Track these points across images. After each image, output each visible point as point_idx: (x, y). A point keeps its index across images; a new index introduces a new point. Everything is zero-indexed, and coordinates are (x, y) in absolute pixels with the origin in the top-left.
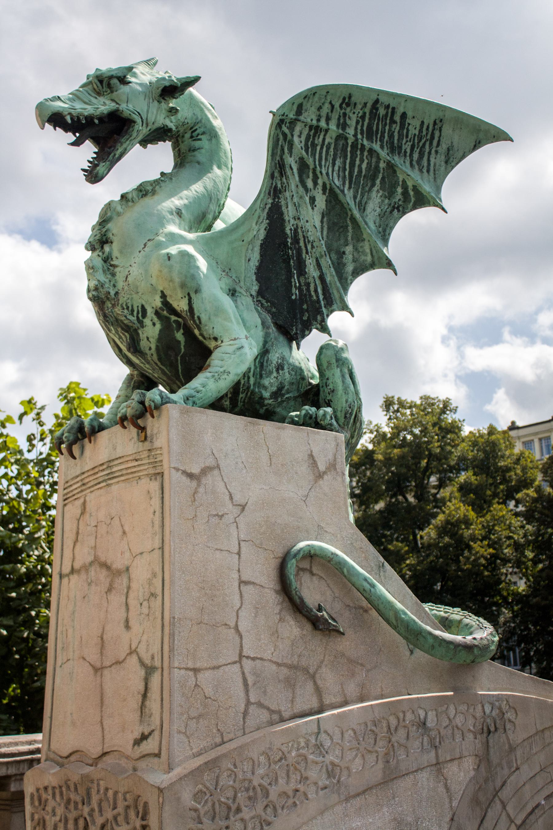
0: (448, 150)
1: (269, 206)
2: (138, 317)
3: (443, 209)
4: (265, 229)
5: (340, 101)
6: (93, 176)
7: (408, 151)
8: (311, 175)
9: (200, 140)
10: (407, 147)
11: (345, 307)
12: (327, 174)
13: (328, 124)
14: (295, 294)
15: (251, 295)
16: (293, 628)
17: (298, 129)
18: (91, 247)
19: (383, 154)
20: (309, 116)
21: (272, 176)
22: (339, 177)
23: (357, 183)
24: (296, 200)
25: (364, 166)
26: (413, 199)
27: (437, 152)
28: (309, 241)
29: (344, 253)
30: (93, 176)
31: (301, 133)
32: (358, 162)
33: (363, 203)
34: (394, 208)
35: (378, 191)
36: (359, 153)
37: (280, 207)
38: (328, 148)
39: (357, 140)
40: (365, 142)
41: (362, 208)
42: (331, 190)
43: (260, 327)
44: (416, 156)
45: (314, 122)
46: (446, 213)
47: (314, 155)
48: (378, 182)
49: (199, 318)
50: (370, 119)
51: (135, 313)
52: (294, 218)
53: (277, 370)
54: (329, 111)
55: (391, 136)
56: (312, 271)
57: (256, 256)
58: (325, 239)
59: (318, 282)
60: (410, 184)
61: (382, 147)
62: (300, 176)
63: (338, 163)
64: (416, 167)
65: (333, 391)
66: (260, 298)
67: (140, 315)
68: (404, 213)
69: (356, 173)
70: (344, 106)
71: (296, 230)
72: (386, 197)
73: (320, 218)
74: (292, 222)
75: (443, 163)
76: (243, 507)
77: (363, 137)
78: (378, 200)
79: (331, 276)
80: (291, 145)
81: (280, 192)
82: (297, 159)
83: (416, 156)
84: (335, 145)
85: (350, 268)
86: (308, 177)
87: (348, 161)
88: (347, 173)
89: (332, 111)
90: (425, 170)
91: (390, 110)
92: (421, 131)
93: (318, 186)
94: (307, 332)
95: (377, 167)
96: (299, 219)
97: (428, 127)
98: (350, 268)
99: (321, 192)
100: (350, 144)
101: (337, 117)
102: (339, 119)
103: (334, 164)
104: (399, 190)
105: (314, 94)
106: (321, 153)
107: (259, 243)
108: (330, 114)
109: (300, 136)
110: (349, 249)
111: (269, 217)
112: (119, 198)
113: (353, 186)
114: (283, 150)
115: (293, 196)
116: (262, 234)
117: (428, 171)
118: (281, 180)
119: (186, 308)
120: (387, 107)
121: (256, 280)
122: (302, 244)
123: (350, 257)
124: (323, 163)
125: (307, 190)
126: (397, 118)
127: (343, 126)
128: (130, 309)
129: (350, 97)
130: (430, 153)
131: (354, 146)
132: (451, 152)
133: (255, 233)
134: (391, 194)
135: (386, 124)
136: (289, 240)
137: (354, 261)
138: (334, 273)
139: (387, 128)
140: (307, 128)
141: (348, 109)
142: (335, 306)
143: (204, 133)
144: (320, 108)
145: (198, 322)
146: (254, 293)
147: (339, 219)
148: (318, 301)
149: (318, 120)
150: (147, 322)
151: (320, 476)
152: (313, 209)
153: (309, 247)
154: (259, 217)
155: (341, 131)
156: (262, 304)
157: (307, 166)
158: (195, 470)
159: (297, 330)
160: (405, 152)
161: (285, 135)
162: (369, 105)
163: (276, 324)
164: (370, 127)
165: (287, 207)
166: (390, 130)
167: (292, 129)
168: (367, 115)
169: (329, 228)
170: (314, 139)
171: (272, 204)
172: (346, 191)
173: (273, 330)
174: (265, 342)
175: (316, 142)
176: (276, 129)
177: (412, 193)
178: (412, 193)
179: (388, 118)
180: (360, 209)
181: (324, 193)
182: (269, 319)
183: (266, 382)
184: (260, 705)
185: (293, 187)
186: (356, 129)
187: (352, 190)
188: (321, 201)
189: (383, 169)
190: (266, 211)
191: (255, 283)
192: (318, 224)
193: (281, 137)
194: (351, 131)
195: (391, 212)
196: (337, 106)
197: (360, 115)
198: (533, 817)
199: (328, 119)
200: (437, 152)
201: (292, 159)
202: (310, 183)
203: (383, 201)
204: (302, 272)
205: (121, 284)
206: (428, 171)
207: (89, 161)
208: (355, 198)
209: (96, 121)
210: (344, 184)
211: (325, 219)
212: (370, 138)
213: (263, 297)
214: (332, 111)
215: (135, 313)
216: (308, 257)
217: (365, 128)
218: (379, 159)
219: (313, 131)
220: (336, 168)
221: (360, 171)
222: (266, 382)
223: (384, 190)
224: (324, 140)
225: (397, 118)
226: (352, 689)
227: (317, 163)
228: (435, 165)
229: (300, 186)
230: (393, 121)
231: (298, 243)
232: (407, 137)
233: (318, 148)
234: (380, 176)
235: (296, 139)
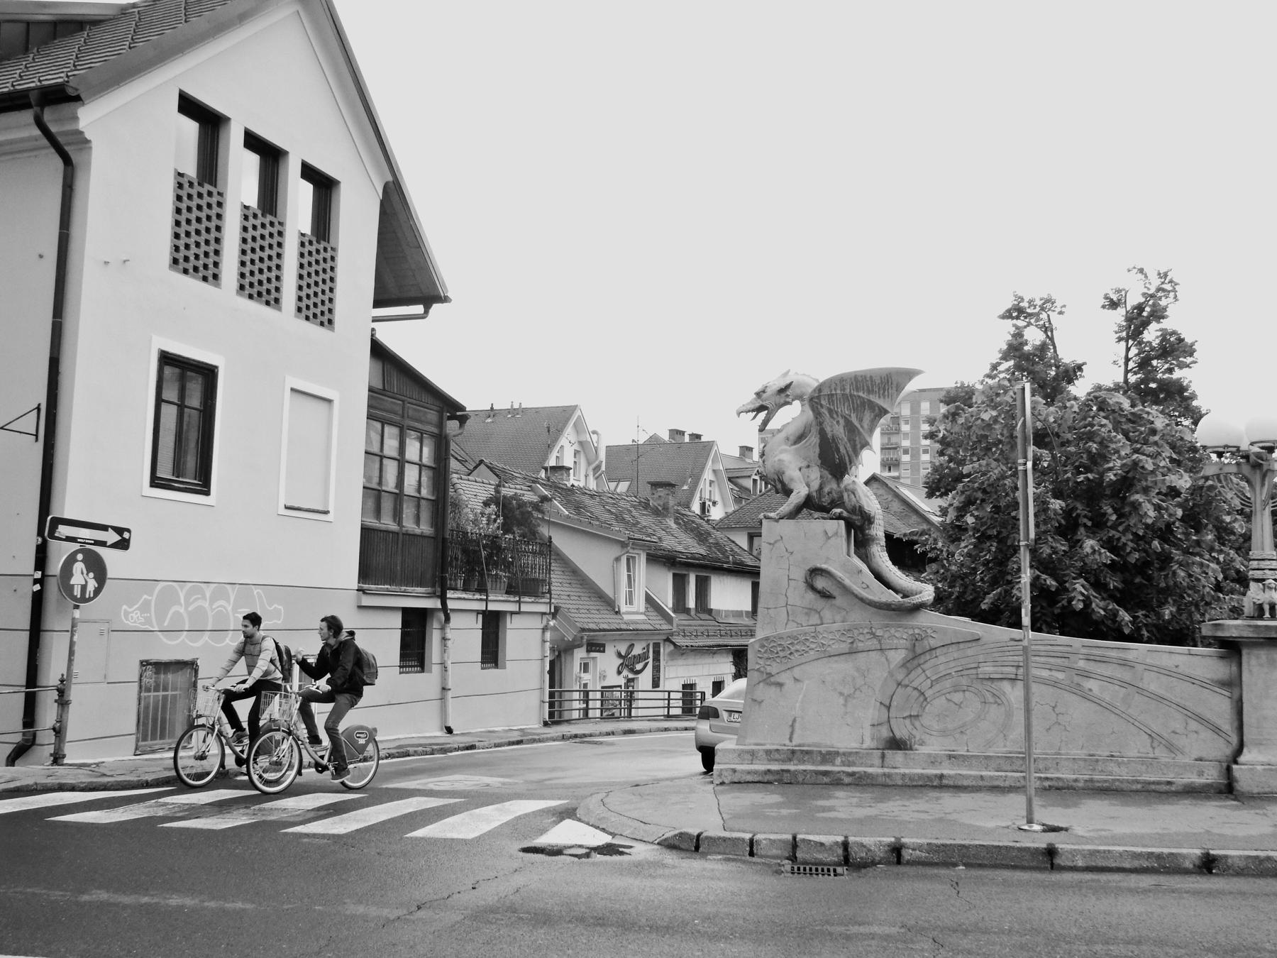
16: (811, 595)
20: (826, 391)
41: (861, 420)
56: (842, 450)
57: (818, 450)
79: (851, 452)
147: (851, 429)
188: (842, 421)
226: (838, 618)
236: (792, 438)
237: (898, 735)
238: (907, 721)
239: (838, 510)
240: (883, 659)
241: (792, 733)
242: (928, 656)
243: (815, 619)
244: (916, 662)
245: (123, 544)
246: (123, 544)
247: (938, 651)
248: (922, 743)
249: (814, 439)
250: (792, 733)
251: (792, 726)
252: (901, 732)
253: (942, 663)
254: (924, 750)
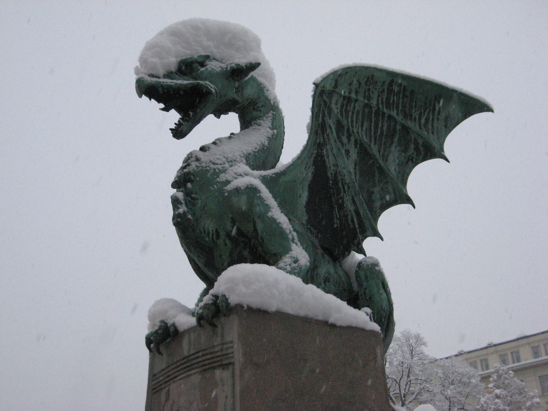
0: (447, 118)
1: (315, 155)
2: (213, 238)
3: (447, 160)
4: (312, 173)
5: (366, 79)
6: (179, 132)
7: (417, 117)
8: (345, 133)
9: (260, 111)
10: (416, 114)
11: (376, 234)
12: (358, 133)
13: (357, 96)
14: (336, 224)
15: (302, 223)
17: (335, 98)
18: (175, 185)
19: (399, 118)
21: (316, 133)
22: (366, 134)
24: (335, 151)
25: (385, 128)
26: (423, 153)
27: (438, 119)
28: (346, 183)
29: (373, 192)
30: (179, 132)
31: (337, 102)
32: (380, 125)
33: (386, 155)
34: (409, 159)
35: (396, 147)
36: (380, 118)
37: (323, 156)
38: (358, 114)
39: (379, 108)
40: (385, 110)
41: (385, 158)
42: (361, 144)
44: (423, 121)
45: (347, 94)
46: (449, 162)
47: (347, 118)
48: (396, 140)
49: (262, 238)
50: (388, 94)
51: (211, 235)
52: (334, 165)
53: (325, 282)
54: (357, 87)
58: (358, 180)
59: (354, 215)
60: (420, 142)
61: (398, 114)
62: (337, 134)
63: (366, 125)
64: (424, 129)
65: (370, 298)
66: (309, 226)
67: (214, 237)
68: (417, 164)
69: (379, 133)
70: (368, 83)
71: (336, 174)
72: (402, 151)
73: (353, 165)
74: (332, 168)
75: (443, 127)
77: (383, 106)
78: (397, 154)
79: (363, 210)
80: (330, 111)
81: (323, 146)
82: (335, 121)
83: (423, 121)
84: (363, 112)
85: (378, 204)
86: (344, 135)
87: (373, 124)
88: (372, 133)
89: (359, 87)
90: (430, 132)
91: (402, 88)
92: (425, 103)
93: (351, 142)
94: (347, 253)
95: (395, 130)
96: (338, 166)
97: (430, 100)
98: (378, 204)
99: (353, 146)
100: (374, 111)
101: (364, 91)
102: (365, 93)
103: (362, 126)
104: (412, 146)
105: (346, 73)
106: (352, 117)
107: (307, 184)
108: (358, 89)
109: (336, 104)
110: (376, 190)
111: (315, 163)
112: (198, 149)
113: (377, 143)
114: (324, 113)
115: (332, 148)
117: (433, 133)
118: (323, 136)
119: (251, 229)
121: (306, 212)
122: (340, 185)
123: (378, 196)
124: (354, 125)
126: (408, 94)
127: (369, 98)
128: (206, 232)
129: (373, 77)
130: (433, 119)
131: (377, 113)
132: (448, 119)
133: (304, 175)
134: (405, 150)
135: (399, 98)
136: (331, 182)
138: (366, 208)
139: (401, 101)
140: (342, 99)
142: (368, 233)
143: (262, 106)
144: (350, 84)
145: (261, 241)
146: (304, 222)
148: (355, 228)
149: (350, 93)
152: (348, 159)
153: (346, 188)
154: (307, 163)
155: (366, 101)
156: (311, 231)
157: (343, 127)
159: (339, 251)
160: (415, 119)
161: (325, 103)
162: (386, 84)
163: (323, 248)
164: (388, 99)
165: (328, 157)
166: (403, 102)
167: (330, 98)
168: (386, 90)
169: (360, 174)
170: (347, 107)
171: (317, 154)
172: (372, 145)
173: (320, 251)
174: (315, 260)
175: (349, 109)
176: (319, 97)
177: (422, 148)
178: (422, 148)
179: (401, 94)
180: (383, 160)
181: (356, 147)
182: (316, 242)
185: (332, 141)
186: (378, 100)
187: (377, 146)
189: (400, 130)
190: (312, 159)
191: (305, 214)
192: (352, 171)
193: (322, 103)
195: (407, 162)
196: (363, 83)
197: (380, 91)
200: (438, 119)
201: (331, 120)
202: (345, 140)
203: (400, 154)
204: (341, 207)
206: (433, 133)
207: (175, 124)
208: (379, 151)
209: (182, 93)
210: (371, 141)
211: (357, 167)
212: (388, 107)
213: (312, 226)
214: (359, 87)
215: (211, 235)
216: (345, 195)
217: (384, 100)
218: (396, 122)
219: (346, 101)
220: (364, 128)
221: (382, 132)
223: (400, 146)
224: (354, 108)
225: (408, 94)
227: (350, 124)
228: (437, 128)
229: (338, 142)
231: (338, 184)
232: (416, 107)
233: (350, 114)
234: (397, 136)
235: (333, 106)
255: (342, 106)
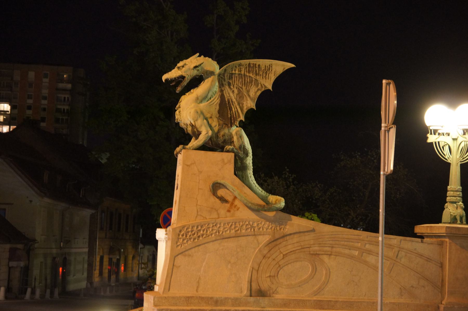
17: (226, 75)
23: (247, 85)
25: (248, 80)
40: (247, 74)
43: (217, 126)
44: (264, 75)
48: (253, 83)
55: (256, 71)
57: (218, 107)
61: (253, 75)
63: (240, 80)
76: (201, 172)
83: (264, 75)
92: (265, 68)
95: (252, 80)
104: (260, 85)
116: (219, 102)
120: (253, 64)
125: (231, 89)
126: (257, 66)
127: (241, 71)
134: (258, 86)
137: (246, 106)
141: (241, 67)
150: (188, 127)
151: (226, 164)
158: (189, 164)
183: (219, 140)
184: (201, 215)
188: (236, 91)
194: (243, 72)
198: (291, 253)
199: (235, 71)
205: (182, 118)
221: (247, 81)
222: (219, 140)
225: (257, 66)
230: (256, 67)
235: (226, 77)
236: (200, 98)
237: (263, 288)
238: (268, 279)
239: (229, 147)
240: (256, 241)
241: (198, 287)
242: (281, 240)
243: (215, 215)
244: (275, 243)
245: (216, 187)
246: (216, 187)
247: (288, 237)
248: (277, 293)
249: (216, 100)
250: (198, 287)
251: (198, 282)
252: (265, 285)
253: (291, 244)
254: (277, 296)
255: (230, 76)
